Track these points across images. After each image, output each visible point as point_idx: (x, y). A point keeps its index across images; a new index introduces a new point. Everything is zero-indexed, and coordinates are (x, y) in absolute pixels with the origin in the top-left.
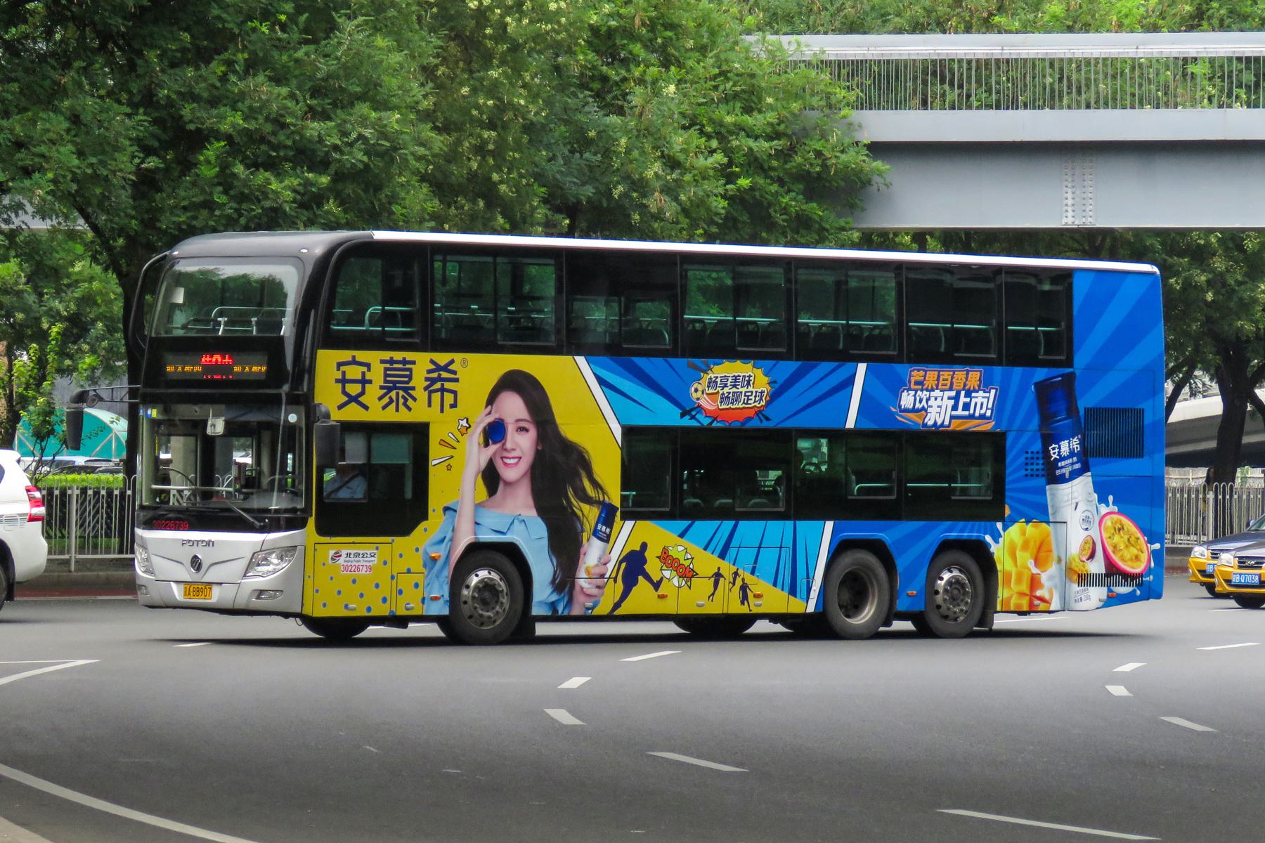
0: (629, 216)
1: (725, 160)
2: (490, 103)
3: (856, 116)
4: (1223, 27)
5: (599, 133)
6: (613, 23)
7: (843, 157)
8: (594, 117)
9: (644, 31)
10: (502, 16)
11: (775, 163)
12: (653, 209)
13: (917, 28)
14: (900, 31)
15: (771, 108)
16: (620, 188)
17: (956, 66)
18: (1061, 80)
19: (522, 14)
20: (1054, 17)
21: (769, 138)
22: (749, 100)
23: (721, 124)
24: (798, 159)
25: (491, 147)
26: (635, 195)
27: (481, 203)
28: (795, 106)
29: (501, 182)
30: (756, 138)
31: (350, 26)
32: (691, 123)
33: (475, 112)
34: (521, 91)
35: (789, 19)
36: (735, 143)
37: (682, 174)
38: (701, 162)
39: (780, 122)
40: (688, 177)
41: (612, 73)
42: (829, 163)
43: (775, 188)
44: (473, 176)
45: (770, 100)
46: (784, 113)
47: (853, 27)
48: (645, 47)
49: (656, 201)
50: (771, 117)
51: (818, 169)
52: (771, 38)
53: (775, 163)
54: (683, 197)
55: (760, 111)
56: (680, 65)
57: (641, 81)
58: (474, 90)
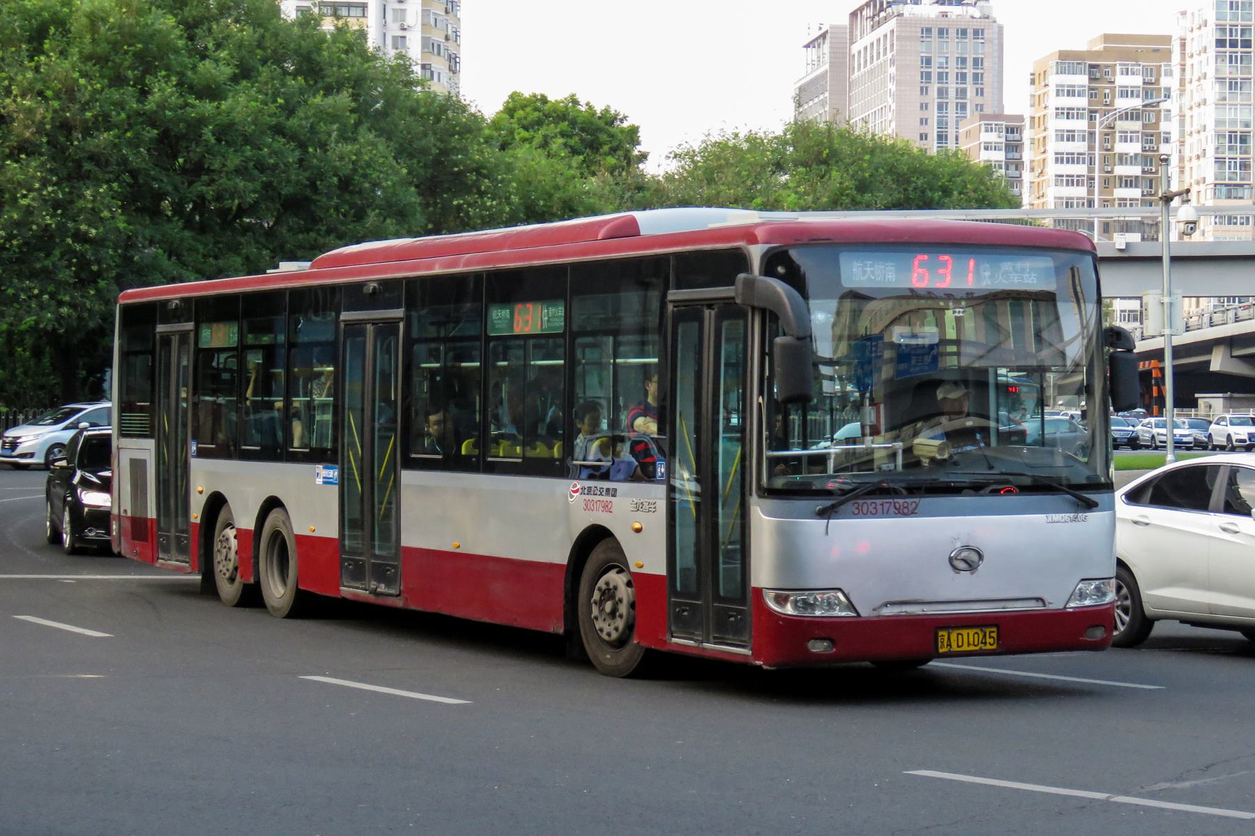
6: (544, 209)
31: (373, 213)
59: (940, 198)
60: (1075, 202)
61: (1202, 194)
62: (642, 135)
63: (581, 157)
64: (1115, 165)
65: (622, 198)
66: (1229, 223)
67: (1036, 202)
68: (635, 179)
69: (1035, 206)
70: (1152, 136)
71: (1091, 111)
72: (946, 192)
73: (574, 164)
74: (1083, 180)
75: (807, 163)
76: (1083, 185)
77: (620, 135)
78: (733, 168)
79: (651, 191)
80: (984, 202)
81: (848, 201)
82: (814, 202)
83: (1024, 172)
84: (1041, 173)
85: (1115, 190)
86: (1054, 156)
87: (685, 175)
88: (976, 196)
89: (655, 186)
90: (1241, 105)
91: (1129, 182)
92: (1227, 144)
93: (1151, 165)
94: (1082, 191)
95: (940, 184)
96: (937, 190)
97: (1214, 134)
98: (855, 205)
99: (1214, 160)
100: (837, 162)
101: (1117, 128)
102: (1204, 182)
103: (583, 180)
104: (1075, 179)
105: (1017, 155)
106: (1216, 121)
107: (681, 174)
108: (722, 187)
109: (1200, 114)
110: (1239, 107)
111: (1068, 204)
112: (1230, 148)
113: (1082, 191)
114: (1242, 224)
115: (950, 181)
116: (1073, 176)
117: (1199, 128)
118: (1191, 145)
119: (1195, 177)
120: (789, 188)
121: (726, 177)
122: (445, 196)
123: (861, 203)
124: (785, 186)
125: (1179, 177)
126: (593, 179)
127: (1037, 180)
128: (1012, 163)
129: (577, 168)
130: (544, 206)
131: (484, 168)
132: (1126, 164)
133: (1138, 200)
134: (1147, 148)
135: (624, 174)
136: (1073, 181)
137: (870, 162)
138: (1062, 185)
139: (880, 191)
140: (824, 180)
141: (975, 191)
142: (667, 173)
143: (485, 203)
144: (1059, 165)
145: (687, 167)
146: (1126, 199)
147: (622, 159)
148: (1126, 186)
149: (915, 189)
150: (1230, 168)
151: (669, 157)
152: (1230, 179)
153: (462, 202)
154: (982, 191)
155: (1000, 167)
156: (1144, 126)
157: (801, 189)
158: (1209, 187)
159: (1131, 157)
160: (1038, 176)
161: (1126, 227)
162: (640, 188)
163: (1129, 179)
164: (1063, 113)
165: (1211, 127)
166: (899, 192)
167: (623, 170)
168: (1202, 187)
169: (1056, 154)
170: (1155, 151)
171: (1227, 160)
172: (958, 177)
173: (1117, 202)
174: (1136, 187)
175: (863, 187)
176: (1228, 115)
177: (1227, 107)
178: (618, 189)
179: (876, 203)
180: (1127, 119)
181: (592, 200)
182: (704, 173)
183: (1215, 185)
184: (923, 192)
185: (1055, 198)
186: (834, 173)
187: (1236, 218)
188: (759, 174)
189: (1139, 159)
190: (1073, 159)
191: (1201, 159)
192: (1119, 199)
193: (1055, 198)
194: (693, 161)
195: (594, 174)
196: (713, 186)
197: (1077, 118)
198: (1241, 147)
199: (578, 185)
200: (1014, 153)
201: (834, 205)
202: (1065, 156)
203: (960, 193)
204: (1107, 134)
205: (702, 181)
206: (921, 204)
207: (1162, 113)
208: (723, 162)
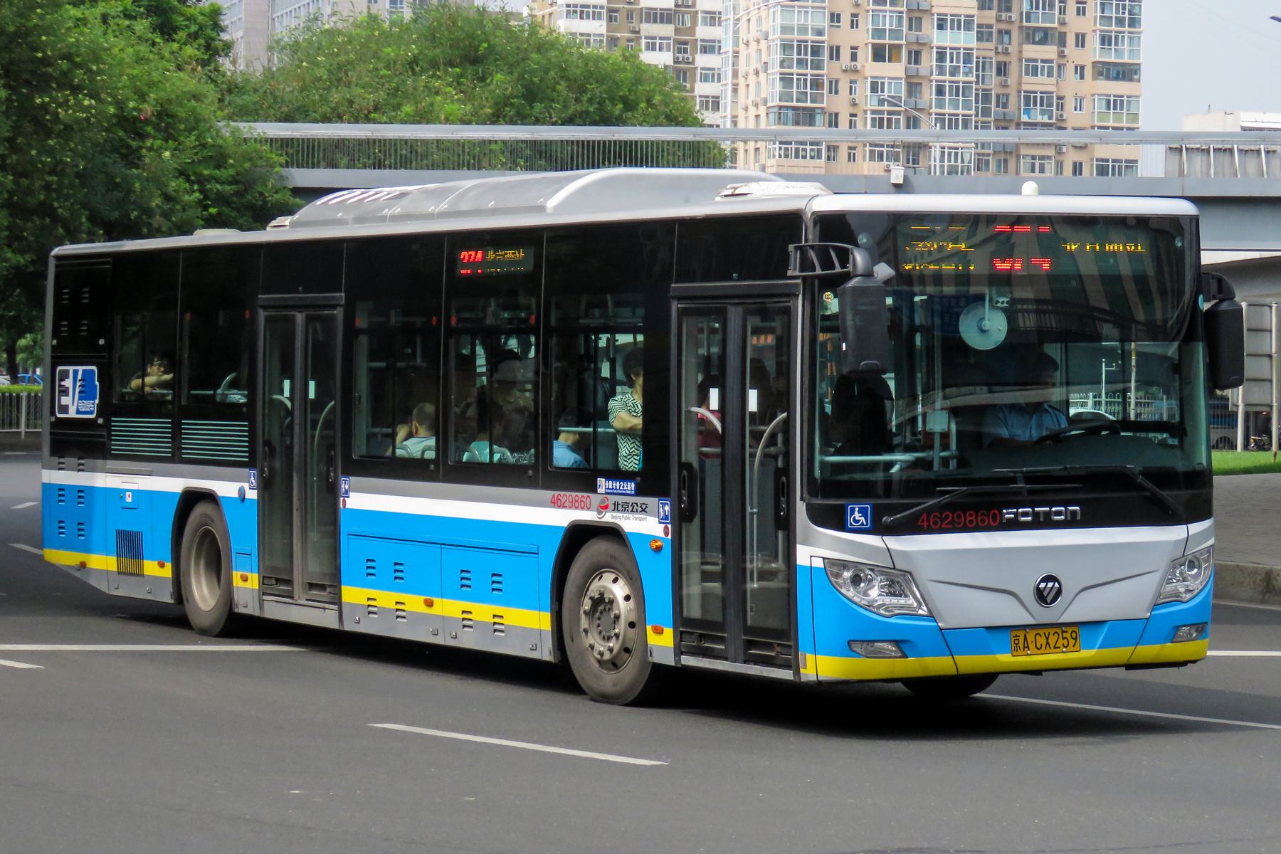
0: (141, 230)
1: (201, 197)
2: (49, 159)
3: (285, 171)
4: (512, 122)
5: (123, 179)
7: (277, 196)
8: (120, 170)
9: (154, 119)
10: (56, 108)
11: (235, 199)
12: (155, 225)
13: (326, 119)
14: (315, 121)
15: (232, 166)
16: (135, 213)
18: (411, 152)
19: (69, 107)
20: (407, 115)
21: (230, 183)
22: (219, 160)
23: (201, 175)
24: (249, 197)
25: (54, 186)
26: (144, 217)
27: (48, 220)
28: (247, 165)
29: (60, 207)
30: (222, 183)
32: (182, 173)
33: (40, 166)
34: (69, 153)
35: (247, 114)
36: (209, 186)
37: (174, 205)
38: (186, 197)
39: (238, 174)
40: (178, 207)
41: (134, 144)
43: (234, 214)
44: (42, 204)
45: (231, 161)
46: (241, 169)
47: (288, 118)
48: (154, 128)
49: (157, 220)
50: (232, 172)
51: (261, 203)
52: (232, 124)
53: (235, 199)
54: (174, 219)
55: (225, 168)
56: (175, 140)
57: (150, 149)
58: (39, 153)
62: (225, 21)
66: (797, 157)
70: (686, 43)
71: (611, 10)
77: (200, 18)
90: (812, 7)
92: (795, 57)
93: (685, 80)
97: (779, 43)
98: (521, 118)
99: (778, 76)
101: (643, 33)
102: (765, 103)
106: (781, 27)
109: (760, 19)
110: (810, 10)
112: (800, 62)
114: (812, 157)
117: (759, 35)
118: (748, 56)
119: (752, 97)
122: (24, 91)
125: (732, 97)
130: (134, 109)
131: (78, 56)
134: (681, 59)
143: (79, 103)
150: (798, 88)
152: (798, 101)
153: (47, 100)
156: (677, 31)
158: (771, 110)
164: (575, 12)
165: (776, 36)
170: (689, 63)
171: (795, 77)
176: (796, 20)
177: (796, 9)
180: (655, 21)
184: (601, 103)
187: (805, 150)
191: (762, 76)
197: (594, 19)
198: (811, 60)
204: (630, 40)
207: (700, 15)
208: (352, 56)
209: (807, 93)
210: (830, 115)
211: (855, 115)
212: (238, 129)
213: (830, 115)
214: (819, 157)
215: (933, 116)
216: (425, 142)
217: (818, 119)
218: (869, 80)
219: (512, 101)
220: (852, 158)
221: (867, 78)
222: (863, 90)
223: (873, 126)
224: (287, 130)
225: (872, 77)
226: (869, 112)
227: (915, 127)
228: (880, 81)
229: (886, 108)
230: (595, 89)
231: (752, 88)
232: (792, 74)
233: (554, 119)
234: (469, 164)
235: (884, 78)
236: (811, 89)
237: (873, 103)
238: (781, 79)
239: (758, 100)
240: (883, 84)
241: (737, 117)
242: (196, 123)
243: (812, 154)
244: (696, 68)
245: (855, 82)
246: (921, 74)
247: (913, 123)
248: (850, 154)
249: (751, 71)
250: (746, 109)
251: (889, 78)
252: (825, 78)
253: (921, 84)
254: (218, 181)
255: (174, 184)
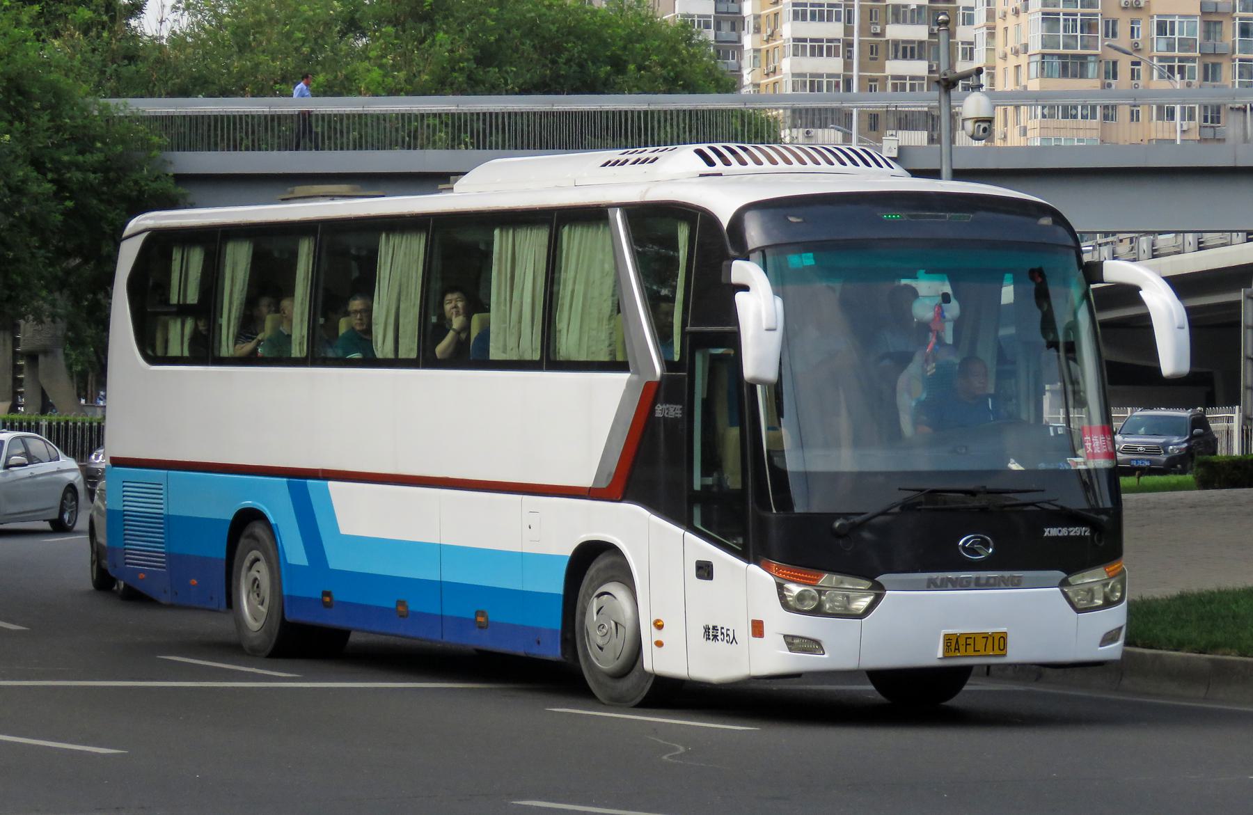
1: (54, 188)
7: (154, 185)
11: (105, 189)
13: (225, 93)
15: (100, 150)
17: (250, 120)
23: (59, 161)
36: (68, 175)
38: (34, 188)
40: (25, 200)
42: (143, 189)
47: (184, 92)
50: (98, 157)
51: (135, 193)
53: (105, 189)
54: (17, 214)
55: (92, 153)
59: (608, 75)
60: (825, 81)
61: (1024, 69)
63: (37, 8)
64: (887, 23)
65: (103, 72)
67: (764, 81)
68: (124, 43)
69: (763, 89)
72: (618, 65)
73: (25, 18)
74: (837, 48)
75: (397, 19)
76: (837, 55)
78: (278, 28)
79: (151, 59)
80: (678, 83)
81: (461, 78)
82: (408, 81)
83: (743, 33)
84: (772, 35)
85: (887, 63)
86: (791, 9)
87: (203, 36)
88: (664, 72)
89: (156, 53)
91: (908, 50)
94: (834, 65)
95: (608, 53)
96: (606, 64)
98: (474, 86)
99: (1040, 16)
100: (446, 17)
102: (1026, 51)
103: (41, 44)
104: (825, 45)
105: (733, 7)
107: (196, 36)
108: (262, 58)
111: (814, 83)
113: (834, 65)
115: (625, 48)
116: (821, 40)
119: (1011, 44)
120: (368, 58)
121: (269, 41)
123: (483, 83)
124: (364, 55)
126: (56, 43)
127: (765, 46)
128: (726, 20)
129: (31, 25)
132: (905, 22)
133: (922, 78)
135: (105, 34)
136: (821, 48)
137: (497, 20)
138: (804, 54)
139: (511, 64)
140: (423, 46)
141: (663, 65)
142: (174, 33)
144: (800, 24)
145: (207, 26)
146: (903, 78)
147: (102, 10)
148: (905, 57)
149: (568, 61)
150: (1065, 31)
151: (178, 8)
152: (1066, 47)
154: (674, 65)
155: (707, 26)
157: (389, 60)
158: (1033, 59)
159: (913, 10)
160: (767, 41)
161: (905, 122)
162: (131, 57)
163: (909, 46)
166: (544, 66)
167: (103, 28)
168: (1023, 59)
169: (794, 5)
171: (1061, 17)
172: (638, 41)
173: (890, 83)
174: (920, 58)
175: (486, 57)
178: (97, 58)
179: (506, 84)
181: (54, 76)
182: (234, 33)
183: (1043, 56)
185: (793, 75)
186: (441, 36)
188: (322, 36)
189: (925, 14)
190: (821, 13)
191: (1022, 15)
192: (894, 77)
193: (793, 75)
194: (216, 15)
195: (57, 35)
196: (248, 55)
199: (32, 53)
200: (730, 4)
201: (441, 86)
202: (809, 9)
203: (640, 68)
205: (229, 47)
206: (578, 84)
208: (263, 16)
209: (1077, 36)
210: (1107, 63)
211: (1138, 64)
212: (107, 107)
213: (1107, 63)
214: (1093, 117)
215: (1237, 63)
216: (341, 117)
217: (1092, 68)
218: (1155, 19)
219: (461, 65)
220: (1134, 116)
221: (1152, 17)
222: (1148, 29)
223: (1161, 77)
224: (170, 107)
225: (1158, 16)
226: (1155, 59)
227: (1214, 79)
228: (1168, 20)
229: (1176, 53)
230: (574, 48)
231: (1011, 32)
232: (1059, 14)
233: (510, 87)
234: (403, 142)
235: (1174, 16)
236: (1082, 32)
237: (1159, 47)
238: (1043, 19)
239: (1018, 46)
240: (1172, 23)
241: (994, 68)
242: (57, 100)
243: (1085, 112)
244: (959, 7)
245: (1138, 22)
246: (1219, 10)
247: (1210, 72)
248: (1132, 112)
249: (1010, 11)
250: (1005, 57)
251: (1181, 16)
252: (1099, 17)
253: (1221, 22)
254: (78, 167)
255: (21, 173)
